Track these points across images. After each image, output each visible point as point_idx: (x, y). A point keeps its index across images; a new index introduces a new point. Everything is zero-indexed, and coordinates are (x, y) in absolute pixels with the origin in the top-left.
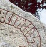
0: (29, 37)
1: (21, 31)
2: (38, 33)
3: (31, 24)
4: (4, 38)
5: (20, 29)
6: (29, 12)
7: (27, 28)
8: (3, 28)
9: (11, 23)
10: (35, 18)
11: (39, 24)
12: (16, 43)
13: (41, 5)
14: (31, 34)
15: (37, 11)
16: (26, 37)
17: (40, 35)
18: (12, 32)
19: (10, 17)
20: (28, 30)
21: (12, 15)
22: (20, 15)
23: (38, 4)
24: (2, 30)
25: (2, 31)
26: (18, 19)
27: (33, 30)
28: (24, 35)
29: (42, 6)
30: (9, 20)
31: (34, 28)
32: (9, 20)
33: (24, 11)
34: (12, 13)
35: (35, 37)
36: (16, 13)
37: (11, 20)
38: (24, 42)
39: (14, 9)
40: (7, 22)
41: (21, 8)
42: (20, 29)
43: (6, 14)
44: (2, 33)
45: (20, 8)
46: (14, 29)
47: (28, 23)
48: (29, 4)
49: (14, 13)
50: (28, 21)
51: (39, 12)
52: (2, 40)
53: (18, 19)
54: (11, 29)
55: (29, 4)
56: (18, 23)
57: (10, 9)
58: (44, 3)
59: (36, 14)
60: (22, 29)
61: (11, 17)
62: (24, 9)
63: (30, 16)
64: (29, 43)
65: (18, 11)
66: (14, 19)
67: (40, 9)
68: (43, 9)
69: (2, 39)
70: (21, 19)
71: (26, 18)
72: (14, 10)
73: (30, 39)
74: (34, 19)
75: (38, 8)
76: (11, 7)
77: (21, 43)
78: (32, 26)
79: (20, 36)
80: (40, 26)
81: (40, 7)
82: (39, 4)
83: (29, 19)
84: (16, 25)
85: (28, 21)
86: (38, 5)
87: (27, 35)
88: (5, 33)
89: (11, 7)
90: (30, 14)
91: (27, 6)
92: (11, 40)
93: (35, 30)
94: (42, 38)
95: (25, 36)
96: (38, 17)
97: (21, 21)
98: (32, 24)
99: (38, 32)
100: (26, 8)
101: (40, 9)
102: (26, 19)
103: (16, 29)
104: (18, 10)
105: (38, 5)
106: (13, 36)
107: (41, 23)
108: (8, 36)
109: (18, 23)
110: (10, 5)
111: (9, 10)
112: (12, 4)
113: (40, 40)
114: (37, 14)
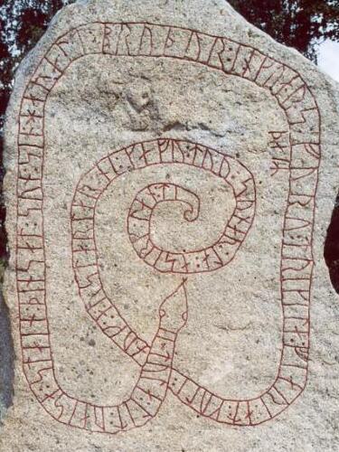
0: (292, 108)
1: (273, 94)
2: (313, 99)
3: (297, 77)
4: (231, 111)
5: (271, 89)
6: (292, 46)
7: (287, 86)
8: (229, 86)
9: (247, 74)
10: (308, 61)
11: (316, 75)
12: (260, 125)
13: (321, 29)
14: (298, 101)
15: (312, 43)
16: (285, 110)
17: (319, 104)
18: (251, 96)
19: (245, 60)
20: (290, 92)
21: (252, 53)
22: (271, 55)
23: (313, 27)
24: (226, 91)
25: (227, 95)
26: (266, 64)
27: (301, 92)
28: (280, 105)
29: (323, 32)
30: (245, 66)
31: (305, 86)
32: (245, 66)
33: (279, 44)
34: (252, 49)
35: (306, 110)
36: (261, 50)
37: (248, 67)
38: (280, 122)
39: (257, 39)
40: (240, 70)
41: (273, 36)
42: (271, 89)
43: (237, 52)
44: (227, 100)
45: (269, 37)
46: (257, 90)
47: (289, 74)
48: (293, 27)
49: (257, 50)
50: (290, 68)
51: (316, 47)
52: (227, 117)
53: (266, 64)
54: (248, 88)
55: (293, 27)
56: (265, 73)
57: (246, 39)
58: (328, 24)
59: (310, 51)
60: (275, 89)
61: (248, 59)
62: (280, 40)
63: (294, 56)
64: (291, 124)
65: (266, 45)
66: (256, 64)
67: (318, 38)
68: (325, 38)
69: (228, 114)
70: (272, 64)
71: (287, 62)
72: (255, 42)
73: (295, 114)
74: (304, 63)
75: (312, 36)
76: (250, 33)
77: (273, 123)
78: (298, 82)
79: (270, 106)
80: (318, 82)
81: (318, 35)
82: (317, 25)
83: (291, 65)
84: (261, 80)
85: (290, 68)
86: (313, 30)
87: (288, 103)
88: (234, 98)
89: (250, 33)
90: (294, 51)
91: (286, 31)
92: (249, 116)
93: (307, 91)
94: (324, 112)
95: (283, 107)
96: (313, 57)
97: (274, 69)
98: (299, 76)
99: (313, 96)
100: (283, 36)
101: (318, 38)
102: (284, 65)
103: (261, 88)
104: (265, 40)
105: (313, 30)
106: (253, 107)
107: (322, 75)
108: (242, 107)
109: (265, 73)
110: (247, 30)
111: (244, 42)
112: (251, 25)
113: (318, 118)
114: (311, 52)
